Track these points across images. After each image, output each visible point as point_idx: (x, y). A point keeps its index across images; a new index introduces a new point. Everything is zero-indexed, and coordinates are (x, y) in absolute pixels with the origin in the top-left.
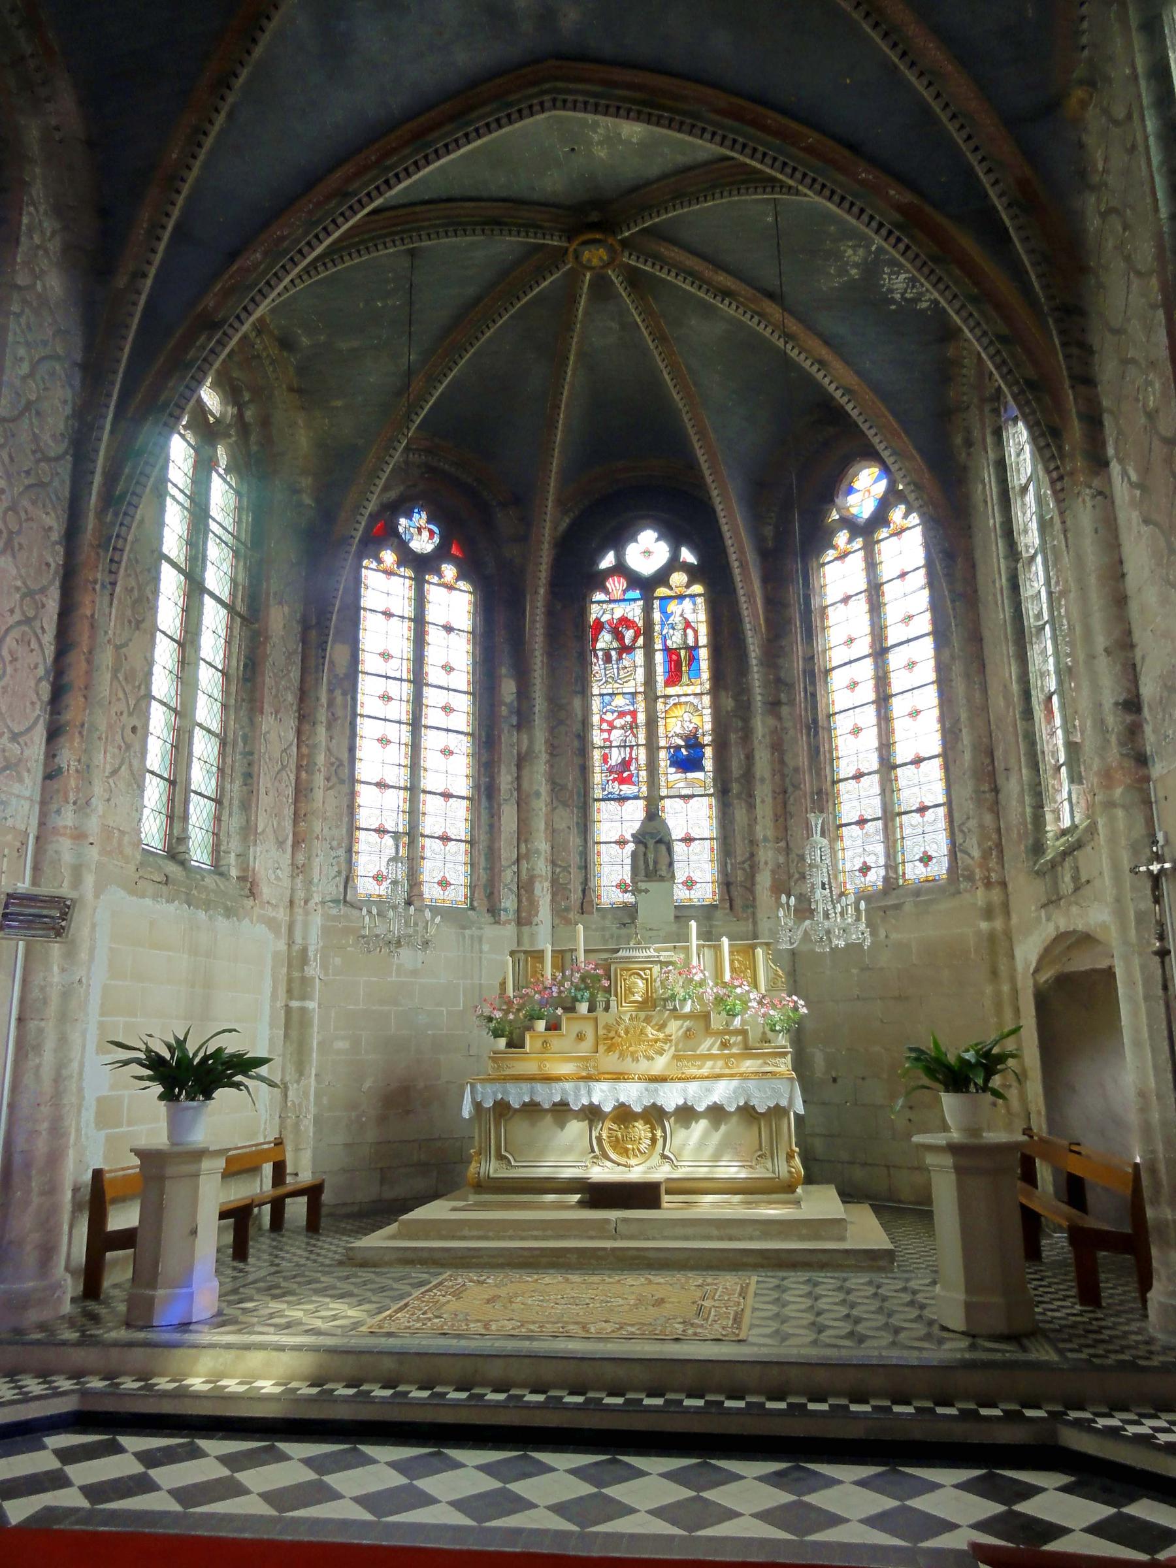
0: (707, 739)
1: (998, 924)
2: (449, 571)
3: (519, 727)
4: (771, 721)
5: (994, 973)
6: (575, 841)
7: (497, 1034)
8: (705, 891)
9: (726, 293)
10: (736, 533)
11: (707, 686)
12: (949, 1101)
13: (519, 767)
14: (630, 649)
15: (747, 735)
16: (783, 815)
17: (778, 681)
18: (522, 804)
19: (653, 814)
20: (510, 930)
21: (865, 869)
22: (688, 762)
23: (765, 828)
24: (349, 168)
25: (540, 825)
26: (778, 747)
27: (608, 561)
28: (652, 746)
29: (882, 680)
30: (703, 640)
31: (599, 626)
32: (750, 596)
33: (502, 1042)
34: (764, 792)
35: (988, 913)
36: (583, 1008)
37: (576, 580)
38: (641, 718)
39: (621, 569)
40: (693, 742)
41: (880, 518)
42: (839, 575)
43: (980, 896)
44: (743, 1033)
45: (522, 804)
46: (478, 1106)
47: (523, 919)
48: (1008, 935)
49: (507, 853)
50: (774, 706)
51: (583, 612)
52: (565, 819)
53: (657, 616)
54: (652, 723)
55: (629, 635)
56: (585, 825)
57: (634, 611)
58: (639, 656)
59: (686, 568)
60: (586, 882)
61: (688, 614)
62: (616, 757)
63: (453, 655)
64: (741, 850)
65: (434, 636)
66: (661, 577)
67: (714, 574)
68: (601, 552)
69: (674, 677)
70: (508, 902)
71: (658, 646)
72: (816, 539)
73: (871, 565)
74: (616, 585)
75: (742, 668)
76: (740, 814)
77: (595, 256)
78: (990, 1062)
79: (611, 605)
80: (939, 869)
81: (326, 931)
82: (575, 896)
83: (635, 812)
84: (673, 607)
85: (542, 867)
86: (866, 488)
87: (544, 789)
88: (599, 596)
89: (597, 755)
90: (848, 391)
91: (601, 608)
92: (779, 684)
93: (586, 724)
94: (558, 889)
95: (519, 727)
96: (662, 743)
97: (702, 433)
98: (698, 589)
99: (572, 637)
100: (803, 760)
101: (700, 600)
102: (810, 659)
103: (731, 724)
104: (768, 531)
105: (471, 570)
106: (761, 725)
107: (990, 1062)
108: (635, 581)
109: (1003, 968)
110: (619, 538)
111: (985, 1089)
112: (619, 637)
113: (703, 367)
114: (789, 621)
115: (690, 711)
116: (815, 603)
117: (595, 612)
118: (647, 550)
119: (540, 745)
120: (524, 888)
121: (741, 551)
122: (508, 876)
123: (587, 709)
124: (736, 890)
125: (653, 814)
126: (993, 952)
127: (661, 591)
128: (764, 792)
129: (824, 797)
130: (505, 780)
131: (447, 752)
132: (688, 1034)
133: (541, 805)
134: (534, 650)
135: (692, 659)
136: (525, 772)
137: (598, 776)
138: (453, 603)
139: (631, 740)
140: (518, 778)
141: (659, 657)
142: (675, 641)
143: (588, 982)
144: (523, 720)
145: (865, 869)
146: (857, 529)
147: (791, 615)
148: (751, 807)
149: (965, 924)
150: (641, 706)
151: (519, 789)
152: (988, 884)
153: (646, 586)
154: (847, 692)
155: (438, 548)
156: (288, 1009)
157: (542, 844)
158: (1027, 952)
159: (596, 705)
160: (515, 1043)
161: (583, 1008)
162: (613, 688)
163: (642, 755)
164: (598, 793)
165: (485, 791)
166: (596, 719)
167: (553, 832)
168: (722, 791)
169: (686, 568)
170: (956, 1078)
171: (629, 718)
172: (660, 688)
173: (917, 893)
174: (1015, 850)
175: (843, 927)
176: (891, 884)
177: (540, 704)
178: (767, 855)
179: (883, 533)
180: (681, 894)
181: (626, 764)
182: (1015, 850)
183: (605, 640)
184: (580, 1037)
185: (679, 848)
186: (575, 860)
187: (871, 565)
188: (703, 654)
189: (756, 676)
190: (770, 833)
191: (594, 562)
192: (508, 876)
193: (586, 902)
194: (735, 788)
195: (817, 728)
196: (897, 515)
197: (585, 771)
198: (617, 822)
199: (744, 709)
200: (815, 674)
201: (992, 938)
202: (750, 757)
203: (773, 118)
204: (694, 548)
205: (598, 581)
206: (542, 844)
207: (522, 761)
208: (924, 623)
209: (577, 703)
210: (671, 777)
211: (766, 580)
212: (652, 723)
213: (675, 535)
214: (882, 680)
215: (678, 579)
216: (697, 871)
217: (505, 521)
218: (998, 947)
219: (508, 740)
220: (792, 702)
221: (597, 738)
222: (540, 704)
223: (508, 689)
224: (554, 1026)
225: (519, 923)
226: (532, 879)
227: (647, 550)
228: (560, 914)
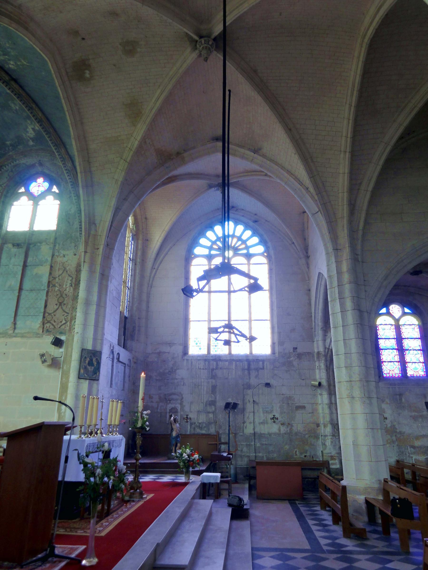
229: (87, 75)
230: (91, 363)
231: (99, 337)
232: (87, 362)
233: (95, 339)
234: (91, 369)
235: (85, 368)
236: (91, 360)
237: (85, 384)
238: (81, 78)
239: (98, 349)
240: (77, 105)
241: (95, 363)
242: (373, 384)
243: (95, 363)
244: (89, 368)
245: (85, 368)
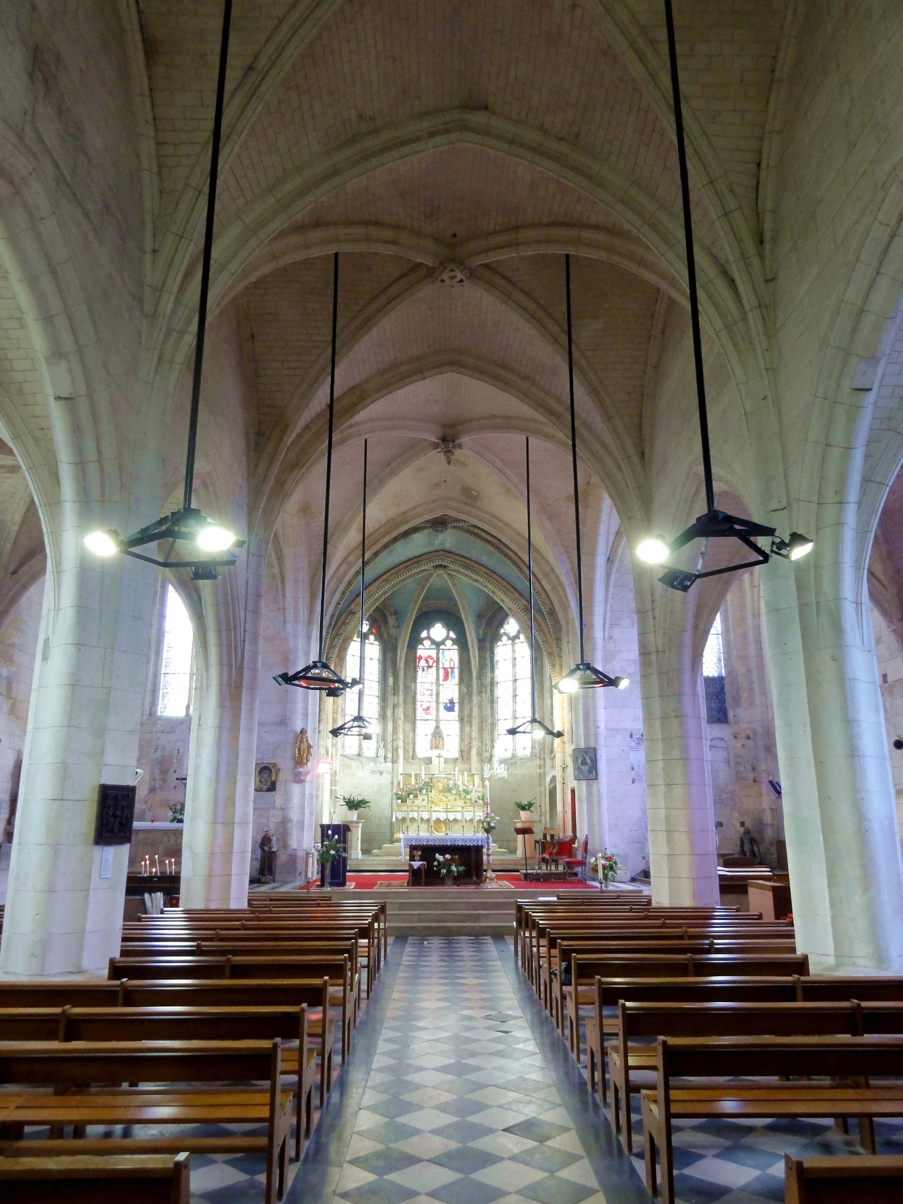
0: (456, 700)
1: (542, 770)
2: (372, 637)
3: (394, 694)
4: (479, 698)
5: (540, 785)
6: (411, 735)
7: (398, 798)
8: (455, 754)
9: (476, 581)
10: (471, 635)
11: (457, 682)
12: (522, 812)
13: (394, 708)
14: (429, 667)
15: (471, 701)
16: (481, 730)
17: (482, 684)
18: (395, 721)
19: (437, 727)
20: (389, 765)
21: (506, 750)
22: (450, 708)
23: (475, 734)
24: (388, 574)
25: (400, 729)
26: (480, 707)
27: (424, 634)
28: (437, 702)
29: (515, 690)
30: (457, 665)
31: (420, 658)
32: (475, 656)
33: (399, 801)
34: (475, 722)
35: (540, 767)
36: (424, 791)
37: (414, 641)
38: (434, 692)
39: (429, 638)
40: (452, 702)
41: (517, 637)
42: (502, 651)
43: (538, 762)
44: (470, 799)
45: (395, 721)
46: (397, 818)
47: (394, 761)
48: (544, 773)
49: (389, 739)
50: (480, 693)
51: (415, 653)
52: (408, 727)
53: (441, 655)
54: (438, 694)
55: (431, 662)
56: (414, 730)
57: (433, 653)
58: (434, 669)
59: (452, 639)
60: (414, 748)
61: (451, 656)
62: (425, 706)
63: (373, 669)
64: (467, 741)
65: (367, 661)
66: (443, 642)
67: (462, 642)
68: (422, 631)
69: (446, 678)
70: (390, 755)
71: (441, 666)
72: (496, 637)
73: (514, 651)
74: (427, 643)
75: (470, 679)
76: (467, 728)
77: (440, 572)
78: (530, 805)
79: (424, 651)
80: (528, 752)
81: (340, 765)
82: (411, 754)
83: (433, 725)
84: (446, 652)
85: (401, 744)
86: (511, 626)
87: (402, 716)
88: (420, 646)
89: (418, 704)
90: (510, 609)
91: (421, 652)
92: (481, 685)
93: (415, 693)
94: (405, 750)
95: (394, 694)
96: (441, 700)
97: (464, 608)
98: (456, 647)
99: (412, 661)
100: (489, 712)
101: (456, 652)
102: (492, 678)
103: (465, 696)
104: (481, 631)
105: (379, 637)
106: (475, 699)
107: (530, 805)
108: (433, 642)
109: (543, 783)
110: (428, 627)
111: (529, 810)
112: (427, 662)
113: (466, 588)
114: (486, 665)
115: (451, 690)
116: (496, 659)
117: (420, 652)
118: (438, 631)
119: (401, 702)
120: (395, 751)
121: (472, 642)
122: (390, 746)
123: (416, 687)
124: (465, 754)
125: (437, 727)
126: (540, 778)
127: (442, 647)
128: (475, 722)
129: (493, 725)
130: (389, 713)
131: (370, 703)
132: (455, 800)
133: (401, 722)
134: (398, 669)
135: (452, 672)
136: (396, 711)
137: (420, 713)
138: (373, 649)
139: (430, 699)
140: (393, 713)
141: (441, 672)
142: (447, 666)
143: (427, 784)
144: (395, 692)
145: (506, 750)
146: (509, 638)
147: (487, 661)
148: (471, 726)
149: (532, 769)
150: (434, 687)
151: (393, 716)
152: (540, 759)
153: (437, 645)
154: (503, 692)
155: (369, 630)
156: (331, 790)
157: (401, 736)
158: (548, 779)
159: (419, 685)
160: (404, 801)
161: (424, 791)
162: (425, 679)
163: (434, 705)
164: (418, 717)
165: (383, 716)
166: (418, 691)
167: (404, 731)
168: (461, 719)
169: (452, 639)
170: (523, 808)
171: (430, 692)
172: (441, 682)
173: (521, 759)
174: (547, 751)
175: (500, 771)
176: (514, 756)
177: (401, 687)
178: (475, 743)
179: (517, 641)
180: (445, 754)
181: (428, 708)
182: (547, 751)
183: (422, 663)
184: (423, 800)
185: (445, 738)
186: (411, 741)
187: (514, 651)
188: (456, 671)
189: (475, 682)
190: (477, 736)
191: (419, 635)
192: (390, 746)
193: (414, 756)
194: (466, 719)
195: (492, 701)
196: (522, 636)
197: (415, 709)
198: (424, 729)
199: (470, 694)
200: (493, 684)
201: (540, 775)
202: (471, 709)
203: (496, 577)
204: (456, 633)
205: (421, 641)
206: (401, 736)
207: (394, 707)
208: (529, 674)
209: (413, 685)
210: (443, 713)
211: (479, 649)
212: (438, 694)
213: (449, 627)
214: (515, 690)
215: (449, 643)
216: (452, 747)
217: (391, 621)
218: (542, 776)
219: (391, 699)
220: (486, 693)
221: (419, 697)
222: (401, 687)
223: (391, 680)
224: (416, 796)
225: (393, 762)
226: (397, 748)
227: (438, 631)
228: (406, 759)
229: (475, 494)
230: (584, 763)
231: (592, 732)
232: (580, 762)
233: (587, 736)
234: (585, 768)
235: (579, 768)
236: (585, 759)
237: (584, 783)
238: (476, 498)
239: (592, 745)
240: (493, 516)
241: (589, 761)
242: (660, 764)
243: (589, 761)
244: (583, 767)
245: (579, 768)
